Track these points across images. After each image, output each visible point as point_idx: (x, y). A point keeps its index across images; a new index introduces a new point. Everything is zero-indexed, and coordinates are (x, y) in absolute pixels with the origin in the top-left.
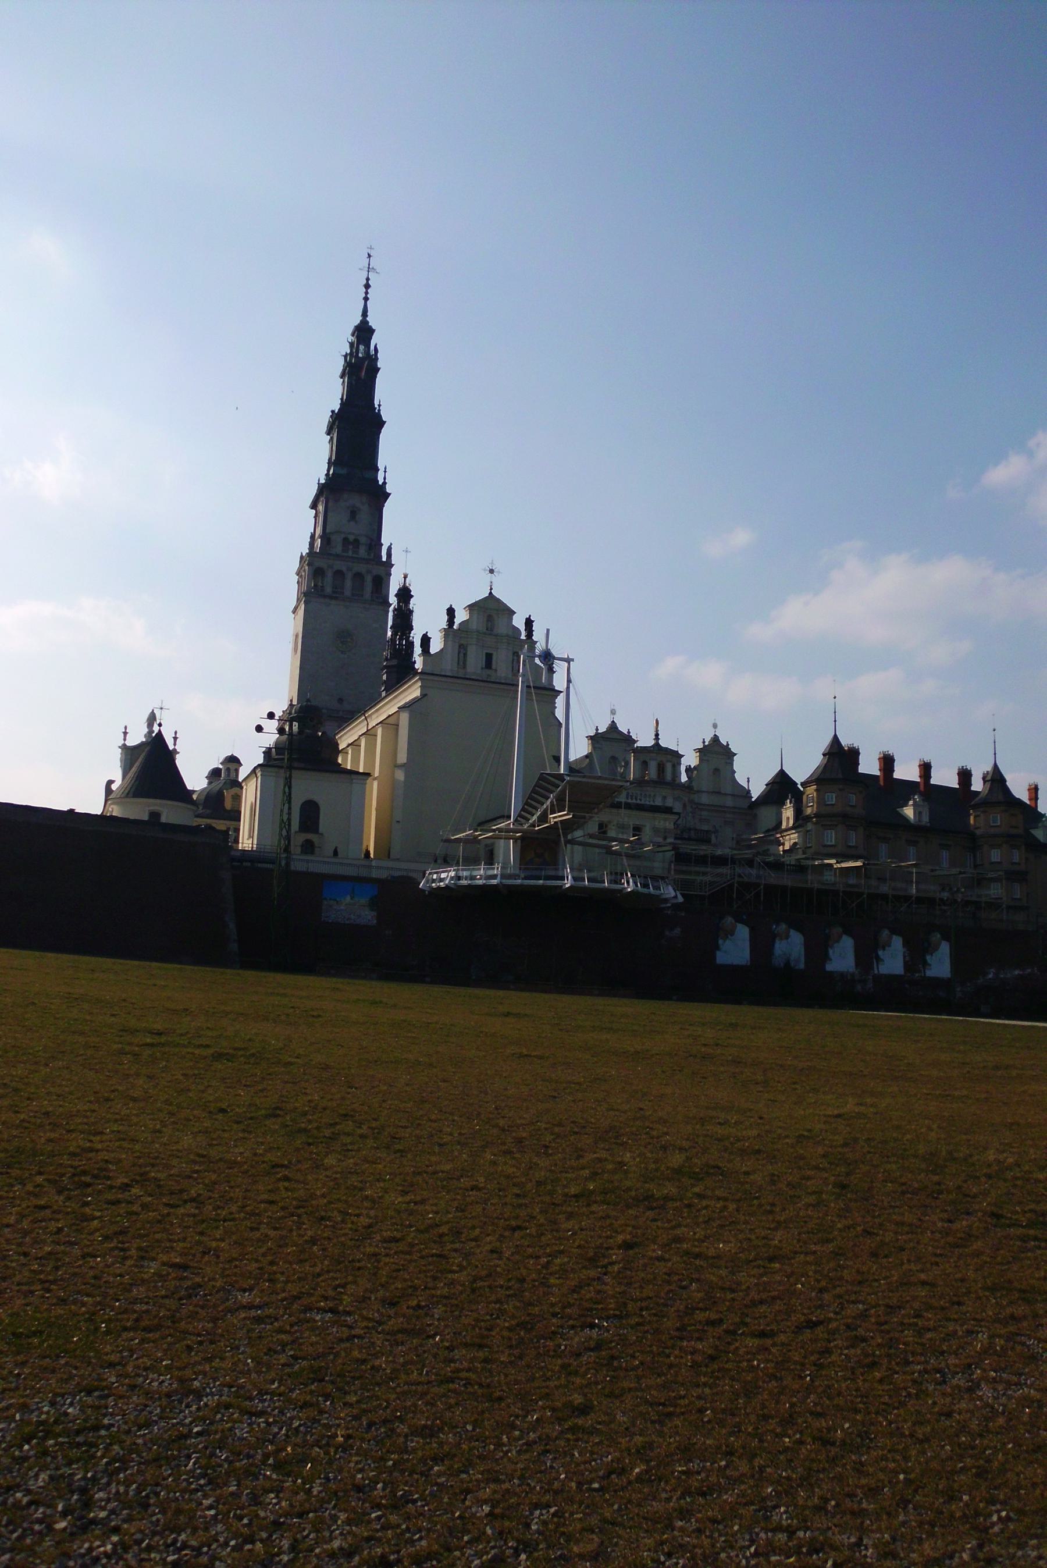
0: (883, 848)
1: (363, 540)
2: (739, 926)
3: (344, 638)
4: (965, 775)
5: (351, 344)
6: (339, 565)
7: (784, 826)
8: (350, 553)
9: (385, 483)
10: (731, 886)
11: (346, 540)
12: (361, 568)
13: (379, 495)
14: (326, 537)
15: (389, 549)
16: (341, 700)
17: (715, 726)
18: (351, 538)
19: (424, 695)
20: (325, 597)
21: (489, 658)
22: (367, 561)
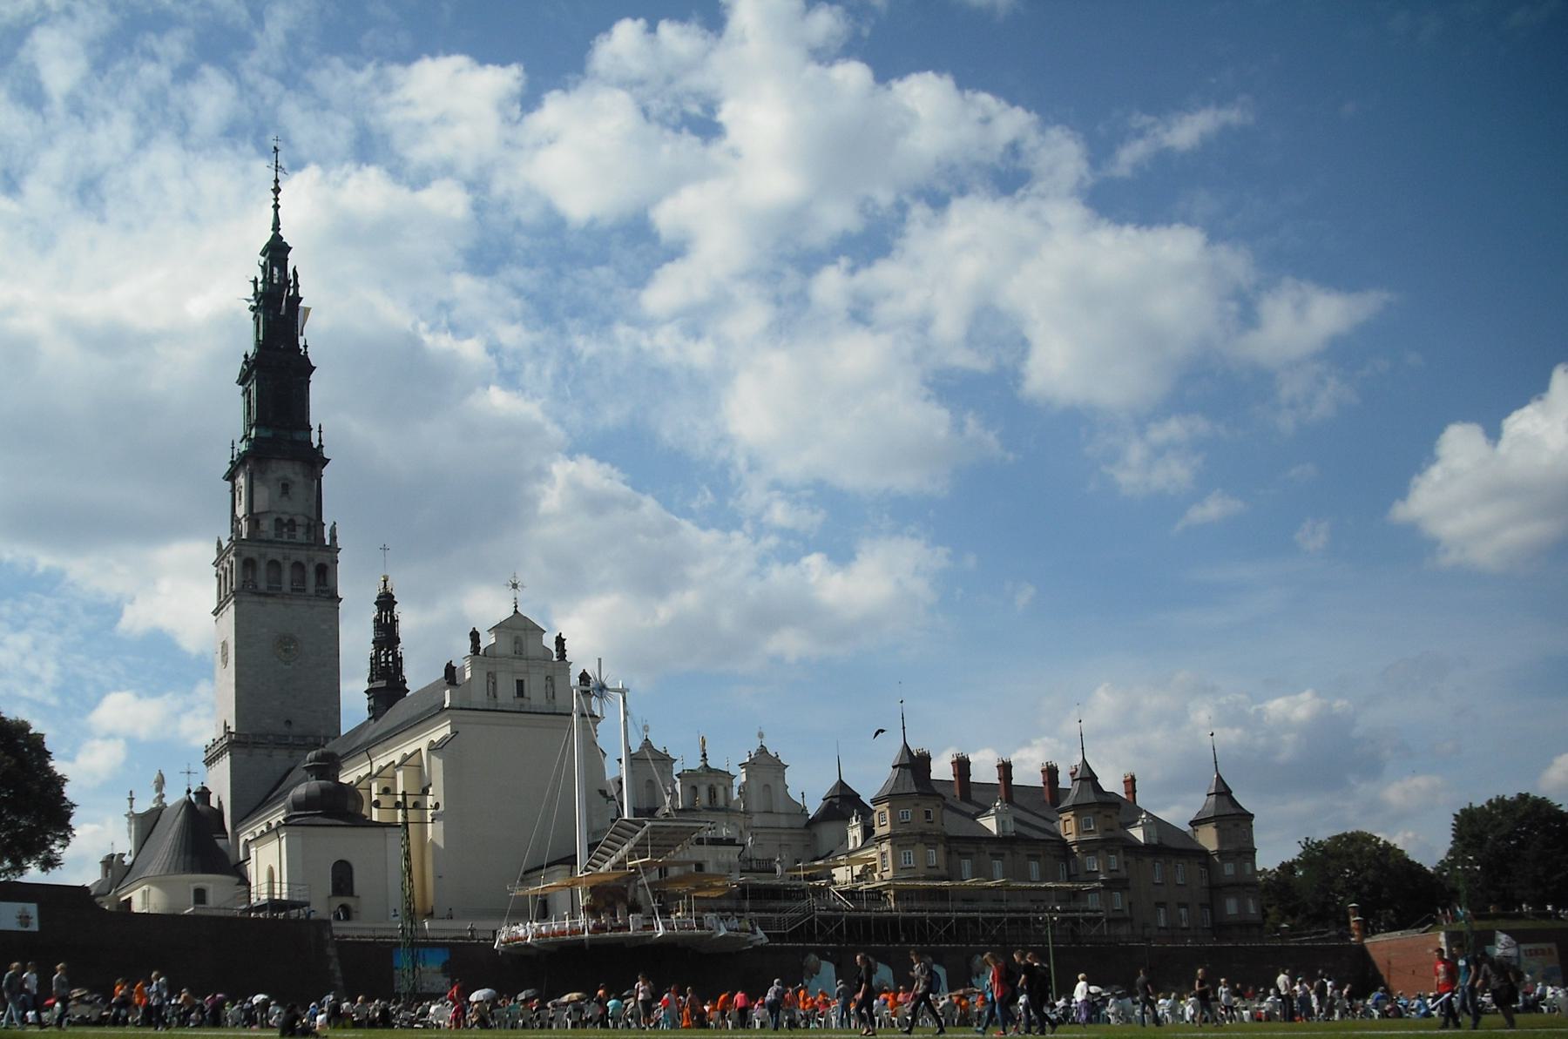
0: (966, 864)
1: (300, 520)
2: (824, 963)
3: (286, 643)
4: (1051, 773)
5: (264, 268)
6: (274, 553)
7: (851, 847)
8: (285, 538)
9: (321, 446)
10: (812, 921)
11: (278, 520)
12: (301, 555)
13: (314, 460)
14: (253, 518)
15: (333, 530)
16: (289, 722)
17: (761, 735)
18: (285, 518)
19: (455, 733)
20: (260, 594)
21: (520, 683)
22: (308, 546)
